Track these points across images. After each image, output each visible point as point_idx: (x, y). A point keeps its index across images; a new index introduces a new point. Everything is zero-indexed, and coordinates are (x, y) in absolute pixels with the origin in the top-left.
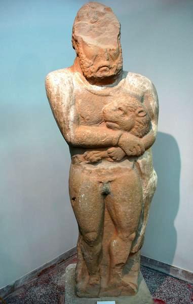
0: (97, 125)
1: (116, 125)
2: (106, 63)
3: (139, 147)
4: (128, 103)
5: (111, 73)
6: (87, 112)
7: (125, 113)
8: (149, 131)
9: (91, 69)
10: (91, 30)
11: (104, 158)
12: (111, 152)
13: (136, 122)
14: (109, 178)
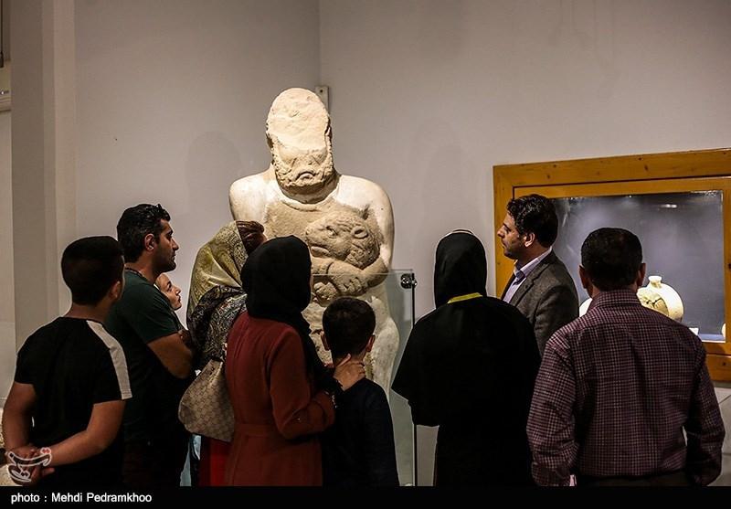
1: (325, 250)
5: (316, 180)
7: (336, 234)
9: (289, 176)
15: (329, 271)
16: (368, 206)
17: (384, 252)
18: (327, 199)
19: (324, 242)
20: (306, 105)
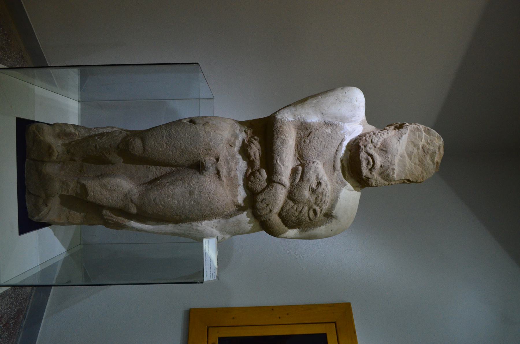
0: (297, 154)
1: (298, 180)
2: (378, 164)
4: (327, 194)
5: (365, 171)
6: (315, 142)
7: (313, 191)
9: (370, 145)
11: (250, 163)
12: (262, 173)
14: (224, 172)
15: (278, 185)
16: (336, 218)
17: (293, 232)
18: (344, 181)
19: (306, 179)
20: (433, 161)
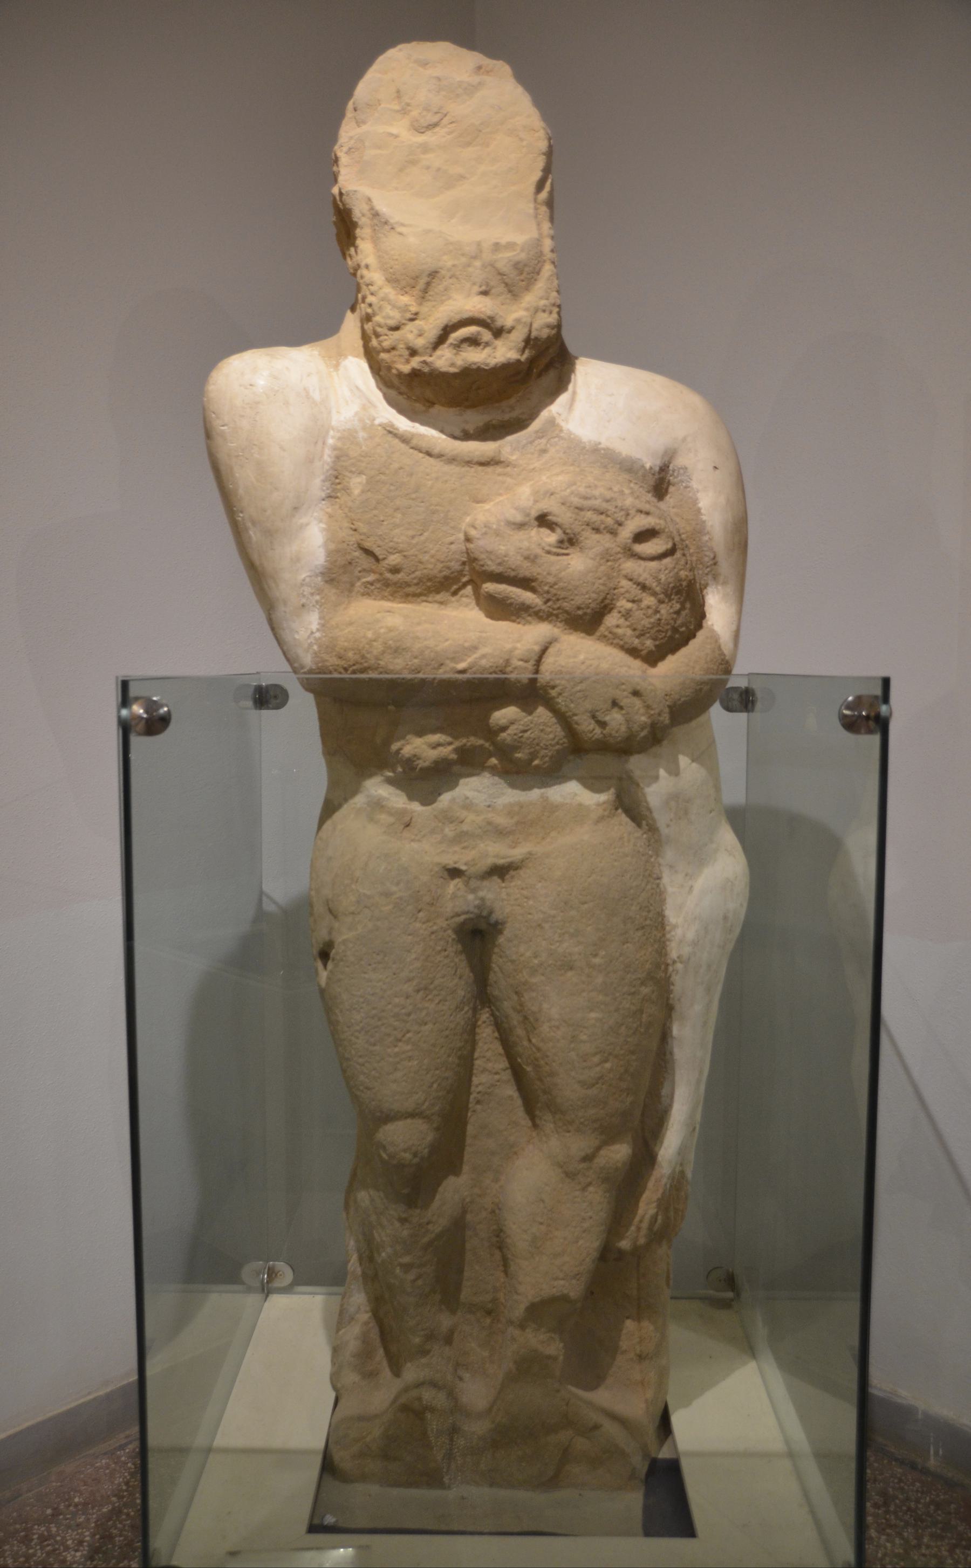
3: (637, 702)
4: (582, 490)
7: (570, 541)
8: (692, 635)
9: (409, 334)
10: (414, 163)
13: (624, 583)
